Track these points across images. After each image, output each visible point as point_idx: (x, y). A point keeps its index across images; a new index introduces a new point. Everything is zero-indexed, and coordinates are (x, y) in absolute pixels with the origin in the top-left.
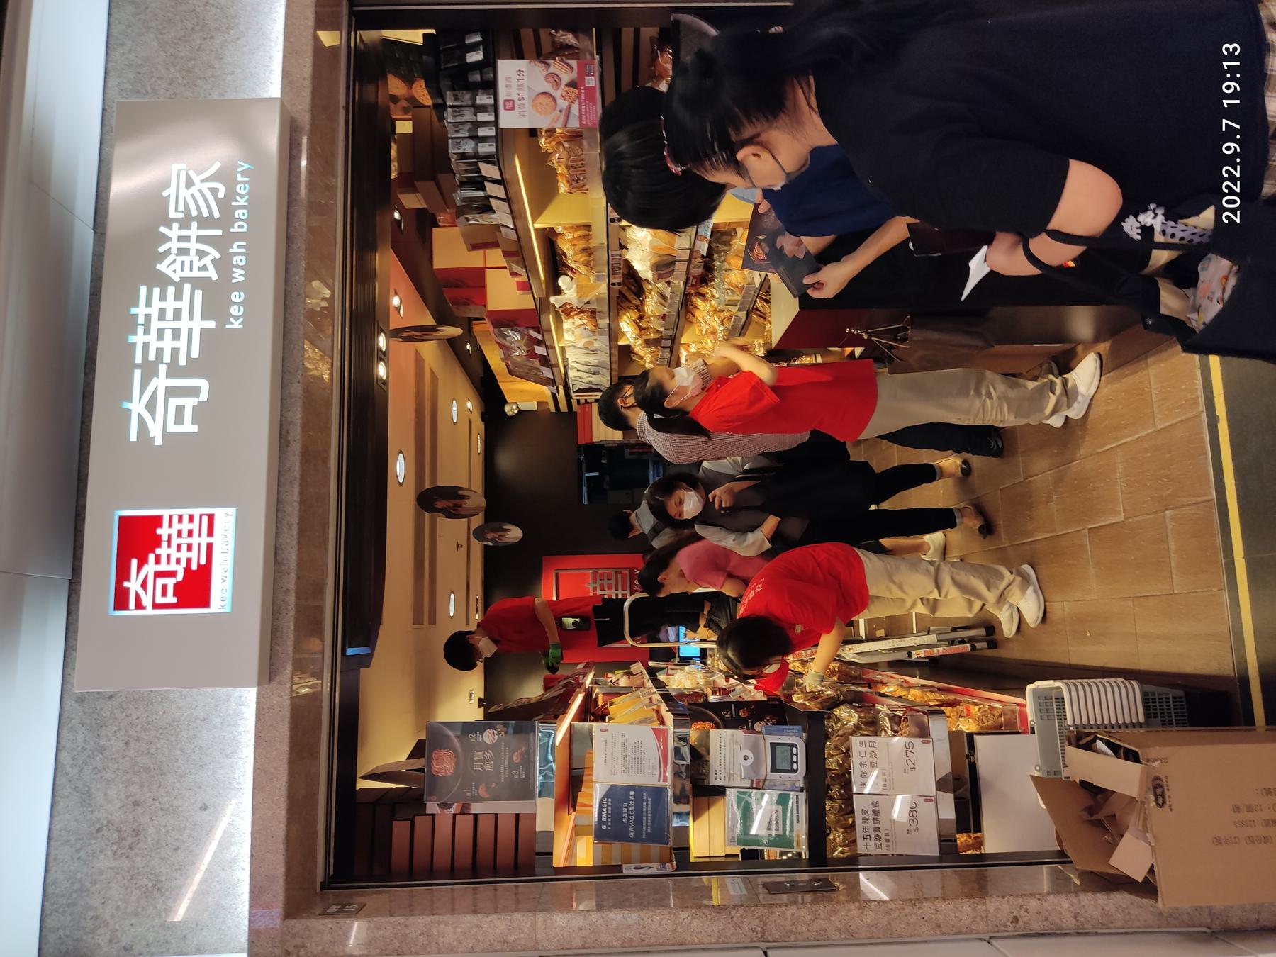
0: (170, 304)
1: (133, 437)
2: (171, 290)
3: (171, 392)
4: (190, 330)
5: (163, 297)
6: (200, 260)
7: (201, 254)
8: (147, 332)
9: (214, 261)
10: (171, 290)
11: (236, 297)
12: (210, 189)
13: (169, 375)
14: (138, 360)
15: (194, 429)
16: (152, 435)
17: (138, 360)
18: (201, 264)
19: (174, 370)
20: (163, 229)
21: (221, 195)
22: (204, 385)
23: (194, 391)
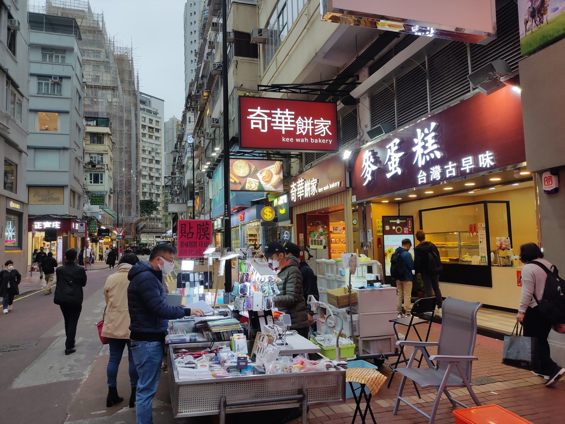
0: (289, 121)
1: (250, 110)
2: (293, 121)
3: (263, 121)
4: (281, 127)
5: (291, 119)
7: (304, 130)
8: (281, 114)
9: (302, 133)
10: (293, 121)
11: (292, 140)
12: (323, 132)
13: (268, 121)
14: (273, 112)
15: (252, 128)
17: (273, 112)
18: (301, 130)
19: (269, 122)
20: (311, 118)
21: (321, 135)
22: (266, 130)
23: (263, 128)
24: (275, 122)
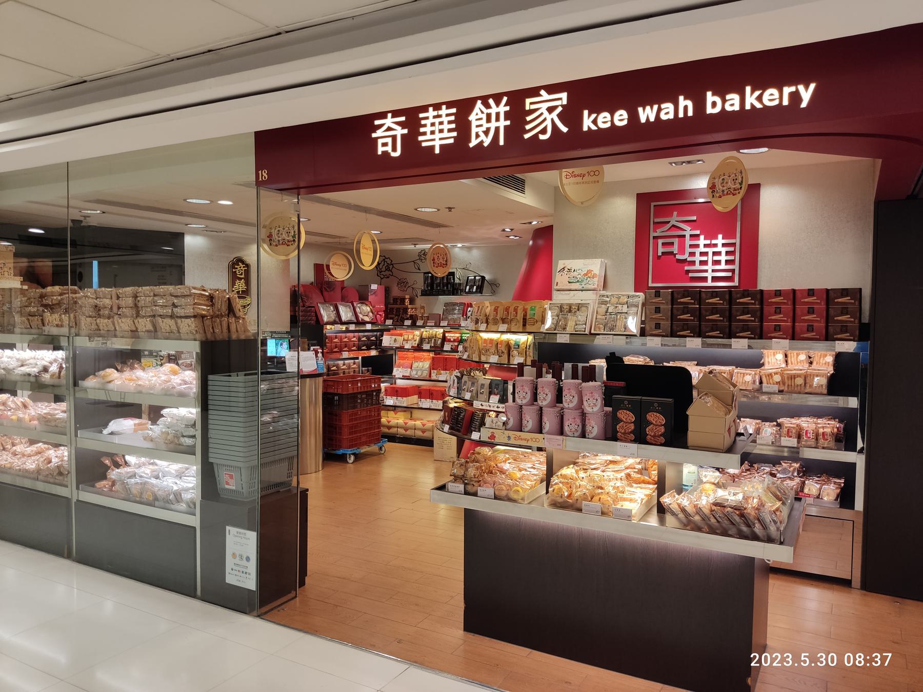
3: (394, 138)
6: (484, 132)
9: (482, 142)
24: (424, 134)
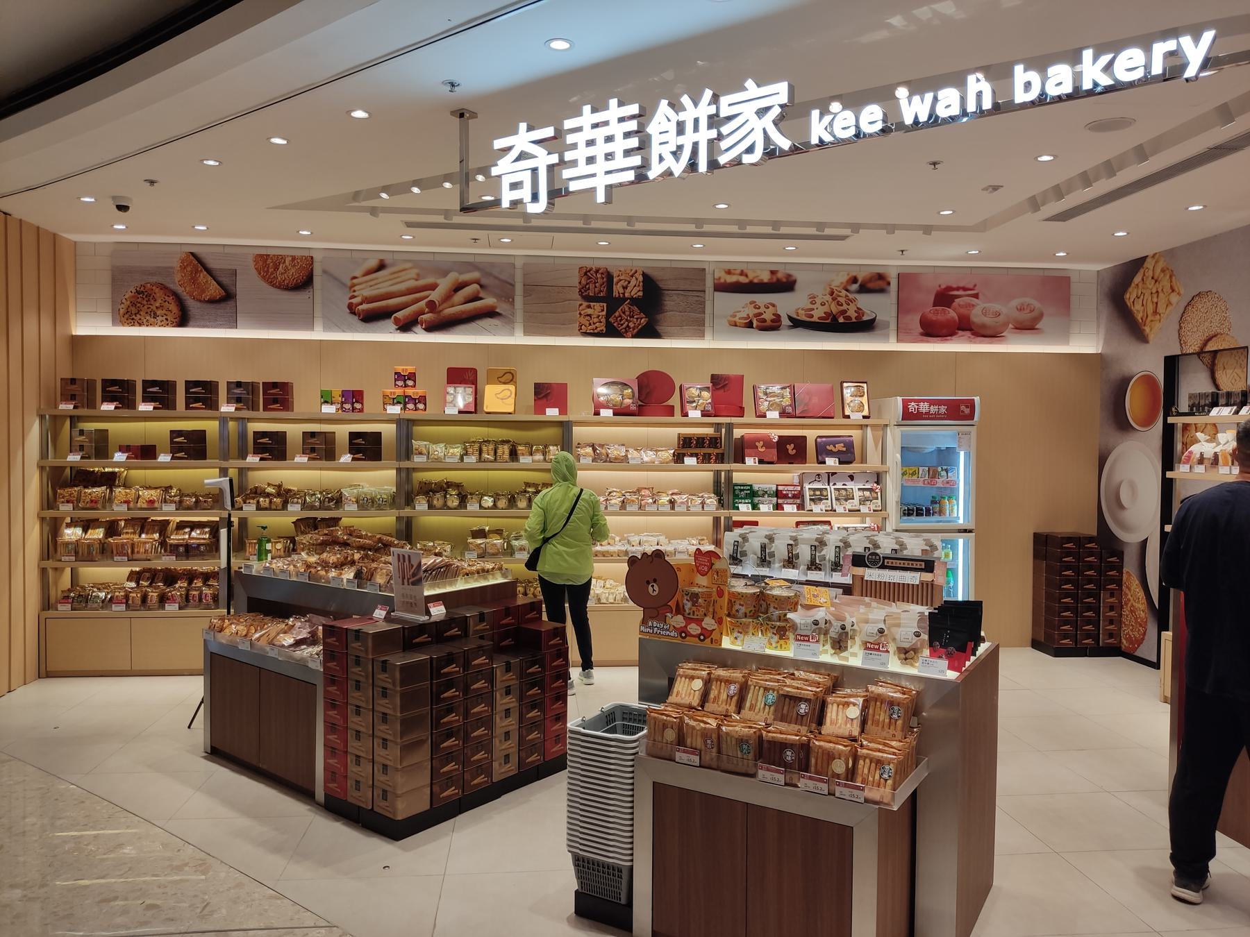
3: (534, 171)
8: (595, 126)
16: (499, 162)
24: (574, 163)
